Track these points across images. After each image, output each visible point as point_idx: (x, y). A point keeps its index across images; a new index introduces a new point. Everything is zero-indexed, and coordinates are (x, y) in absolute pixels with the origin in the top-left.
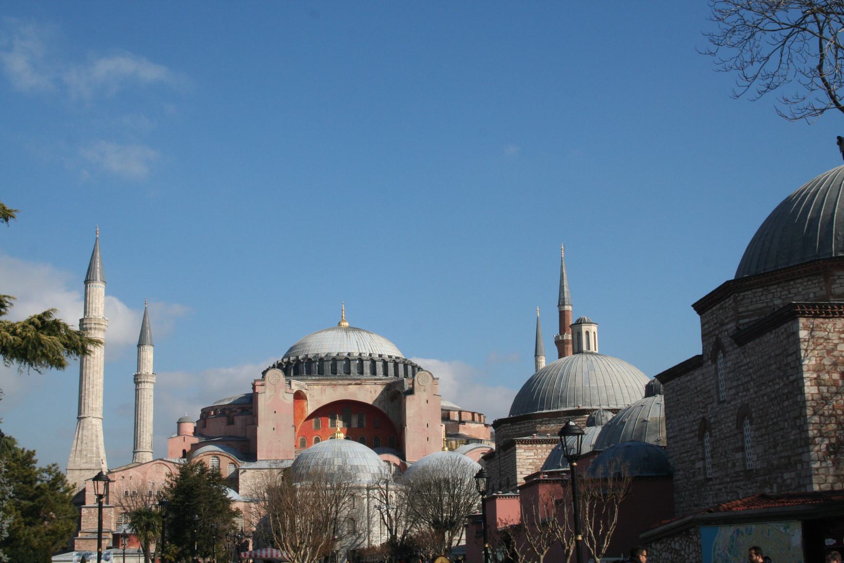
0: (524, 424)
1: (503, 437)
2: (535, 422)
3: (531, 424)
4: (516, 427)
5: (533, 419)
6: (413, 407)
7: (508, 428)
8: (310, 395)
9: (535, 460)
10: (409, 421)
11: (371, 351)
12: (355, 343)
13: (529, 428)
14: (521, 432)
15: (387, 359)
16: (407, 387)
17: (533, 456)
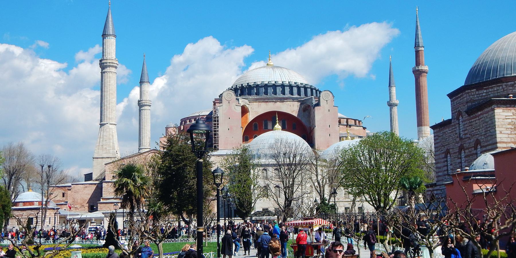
0: (492, 88)
1: (467, 102)
2: (506, 85)
3: (501, 87)
4: (482, 92)
5: (503, 83)
6: (319, 114)
7: (473, 94)
8: (251, 108)
9: (514, 120)
10: (317, 123)
11: (289, 80)
12: (280, 76)
13: (499, 91)
14: (488, 96)
15: (300, 85)
16: (314, 103)
17: (511, 116)
